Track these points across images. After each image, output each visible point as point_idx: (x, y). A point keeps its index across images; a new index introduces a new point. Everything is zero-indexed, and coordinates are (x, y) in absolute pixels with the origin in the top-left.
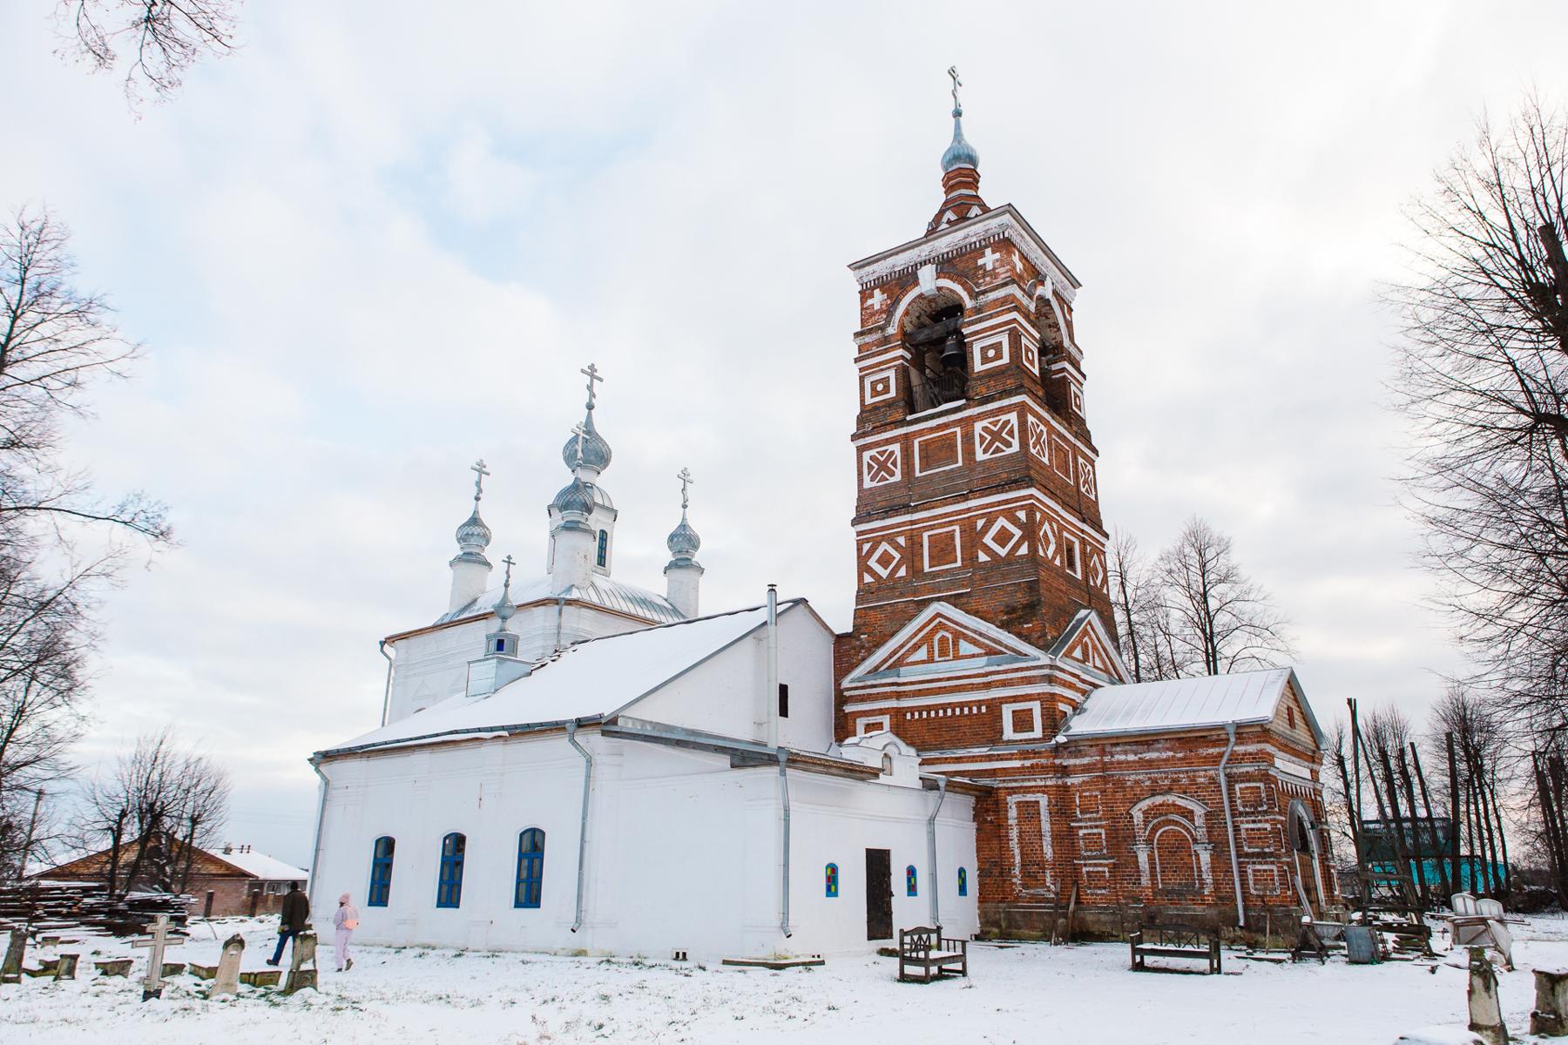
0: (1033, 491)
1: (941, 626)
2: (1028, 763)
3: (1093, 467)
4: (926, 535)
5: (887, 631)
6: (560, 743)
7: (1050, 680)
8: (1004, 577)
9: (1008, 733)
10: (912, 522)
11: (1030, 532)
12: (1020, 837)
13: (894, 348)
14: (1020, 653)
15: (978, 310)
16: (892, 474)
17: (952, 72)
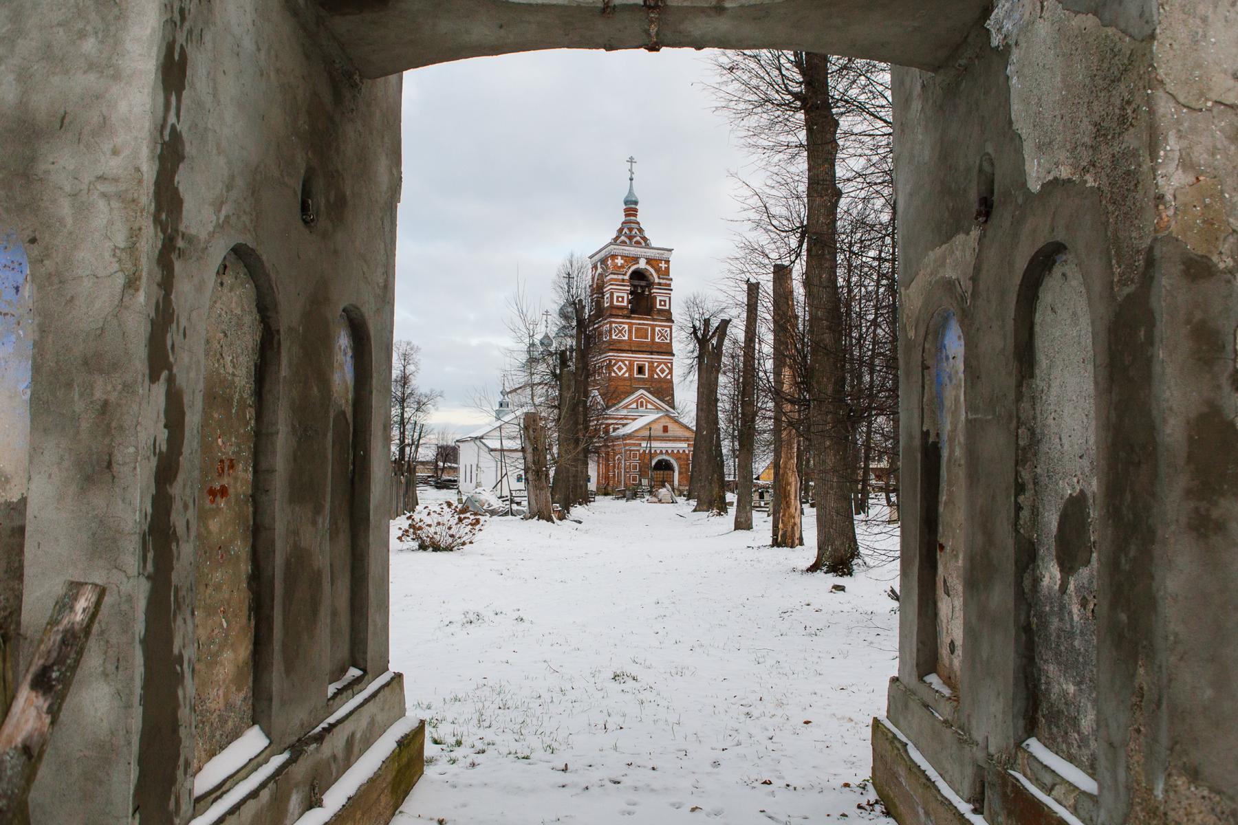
4: (636, 363)
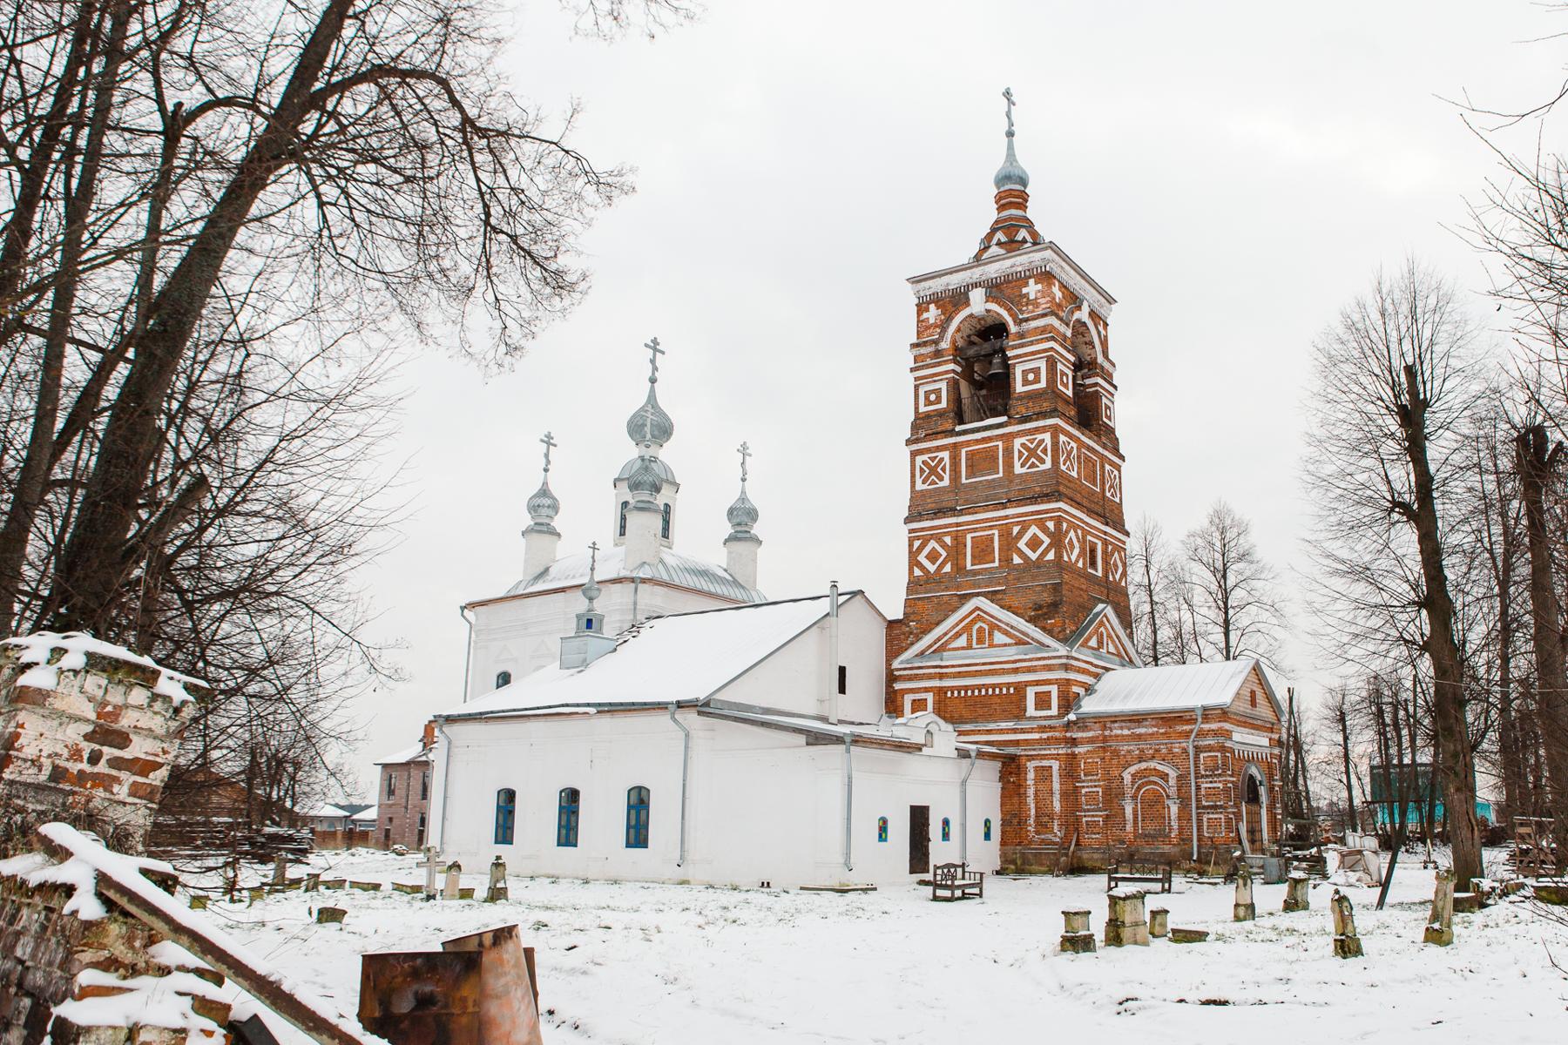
0: (1061, 505)
1: (979, 618)
2: (1045, 736)
3: (1120, 472)
4: (969, 536)
5: (935, 619)
6: (663, 719)
7: (1067, 668)
8: (1034, 578)
9: (1031, 710)
10: (958, 525)
11: (1057, 540)
12: (1036, 794)
13: (946, 362)
14: (1043, 644)
15: (1021, 335)
16: (941, 479)
17: (1007, 94)
